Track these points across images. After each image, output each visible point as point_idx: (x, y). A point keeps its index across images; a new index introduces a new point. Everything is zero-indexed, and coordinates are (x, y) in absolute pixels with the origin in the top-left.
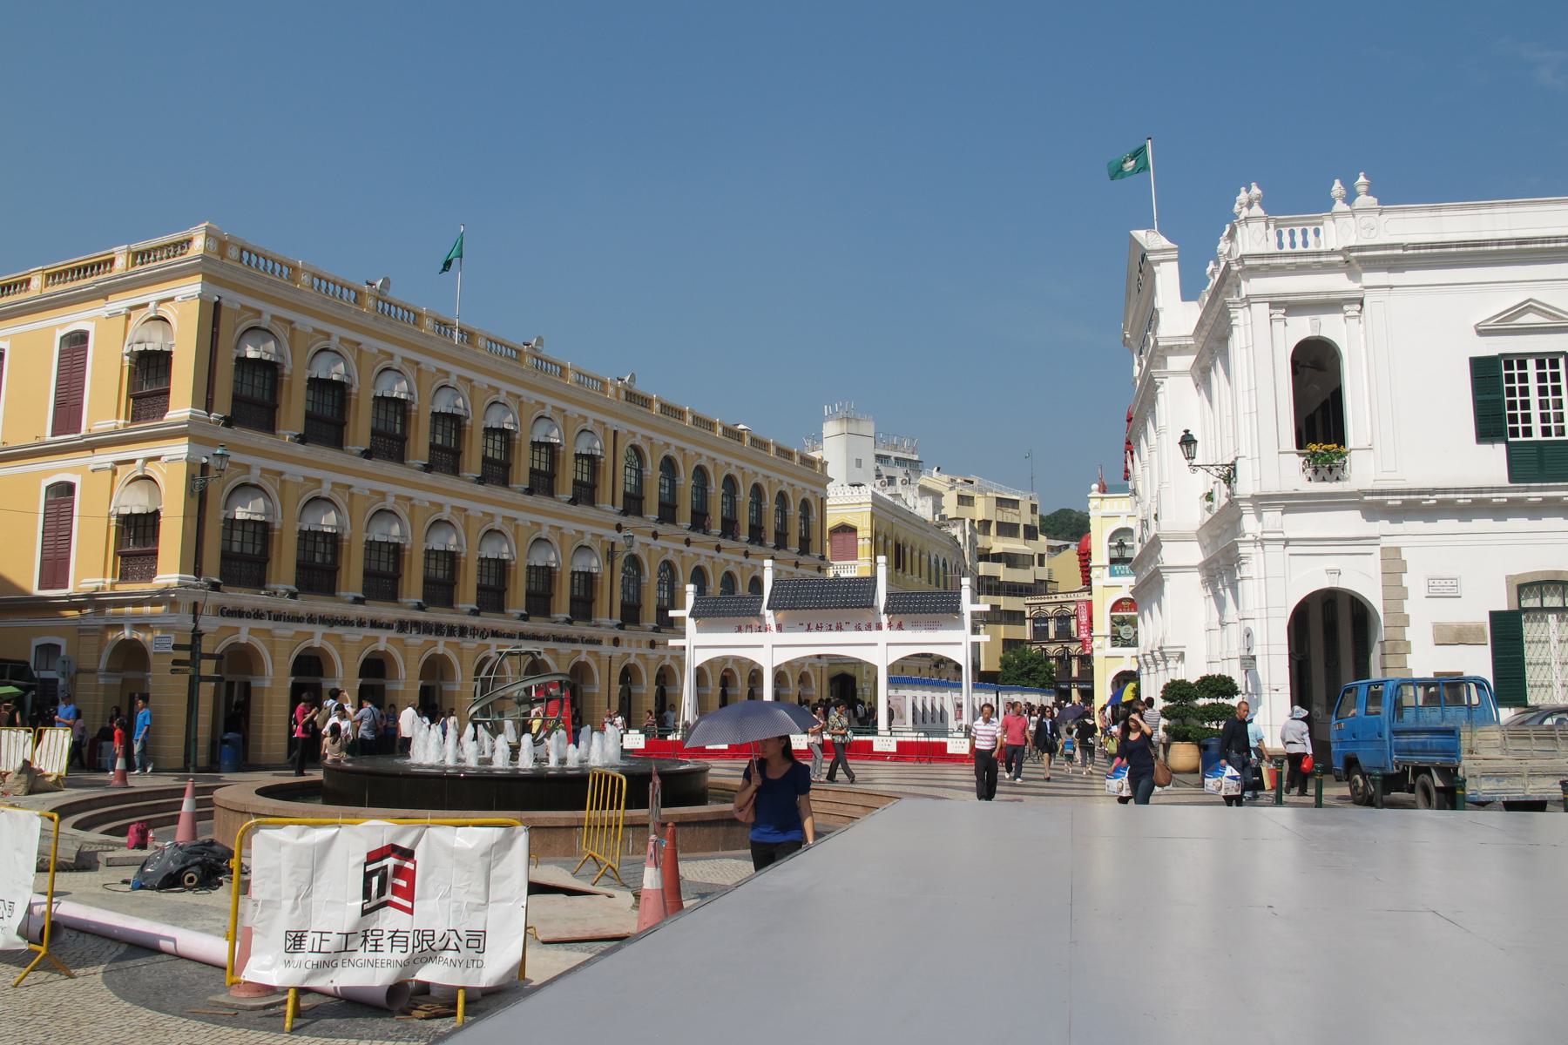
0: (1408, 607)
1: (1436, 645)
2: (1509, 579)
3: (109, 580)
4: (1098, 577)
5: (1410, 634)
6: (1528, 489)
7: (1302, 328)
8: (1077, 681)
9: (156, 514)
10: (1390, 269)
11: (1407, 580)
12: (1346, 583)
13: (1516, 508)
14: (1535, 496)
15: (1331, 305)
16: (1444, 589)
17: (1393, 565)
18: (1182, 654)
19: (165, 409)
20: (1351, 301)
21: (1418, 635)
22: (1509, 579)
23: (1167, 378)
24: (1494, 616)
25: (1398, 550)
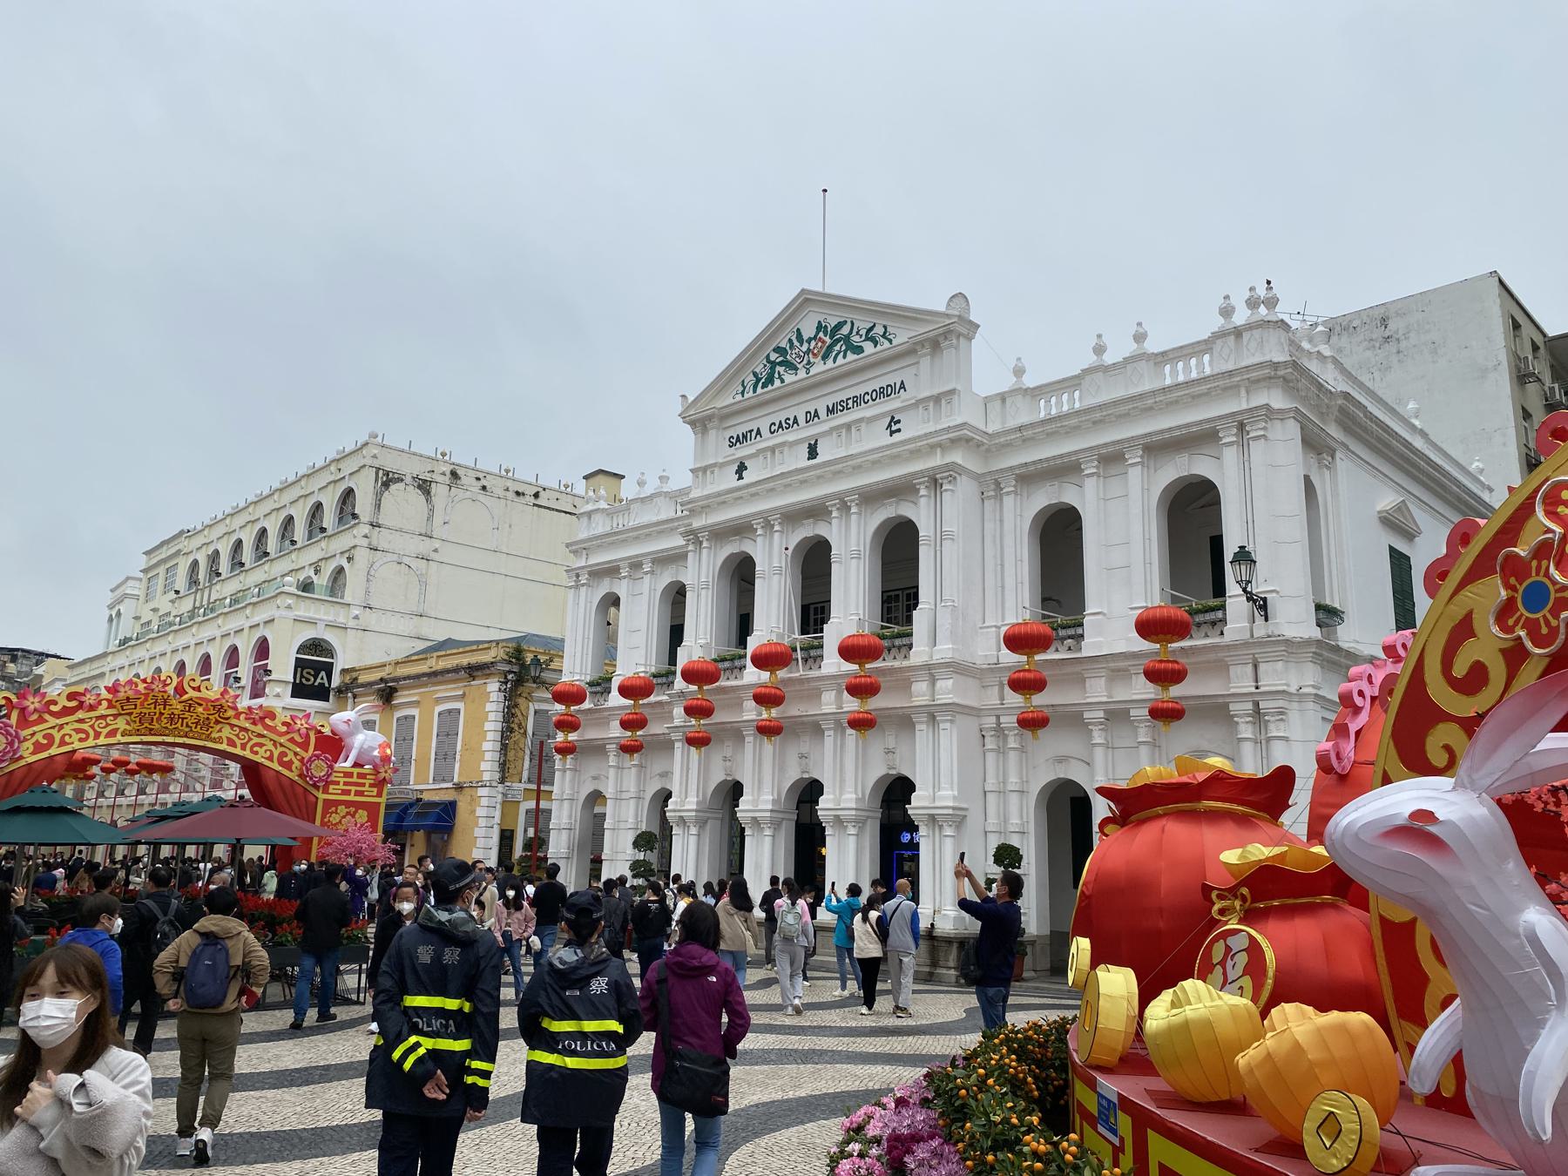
4: (278, 695)
23: (960, 474)
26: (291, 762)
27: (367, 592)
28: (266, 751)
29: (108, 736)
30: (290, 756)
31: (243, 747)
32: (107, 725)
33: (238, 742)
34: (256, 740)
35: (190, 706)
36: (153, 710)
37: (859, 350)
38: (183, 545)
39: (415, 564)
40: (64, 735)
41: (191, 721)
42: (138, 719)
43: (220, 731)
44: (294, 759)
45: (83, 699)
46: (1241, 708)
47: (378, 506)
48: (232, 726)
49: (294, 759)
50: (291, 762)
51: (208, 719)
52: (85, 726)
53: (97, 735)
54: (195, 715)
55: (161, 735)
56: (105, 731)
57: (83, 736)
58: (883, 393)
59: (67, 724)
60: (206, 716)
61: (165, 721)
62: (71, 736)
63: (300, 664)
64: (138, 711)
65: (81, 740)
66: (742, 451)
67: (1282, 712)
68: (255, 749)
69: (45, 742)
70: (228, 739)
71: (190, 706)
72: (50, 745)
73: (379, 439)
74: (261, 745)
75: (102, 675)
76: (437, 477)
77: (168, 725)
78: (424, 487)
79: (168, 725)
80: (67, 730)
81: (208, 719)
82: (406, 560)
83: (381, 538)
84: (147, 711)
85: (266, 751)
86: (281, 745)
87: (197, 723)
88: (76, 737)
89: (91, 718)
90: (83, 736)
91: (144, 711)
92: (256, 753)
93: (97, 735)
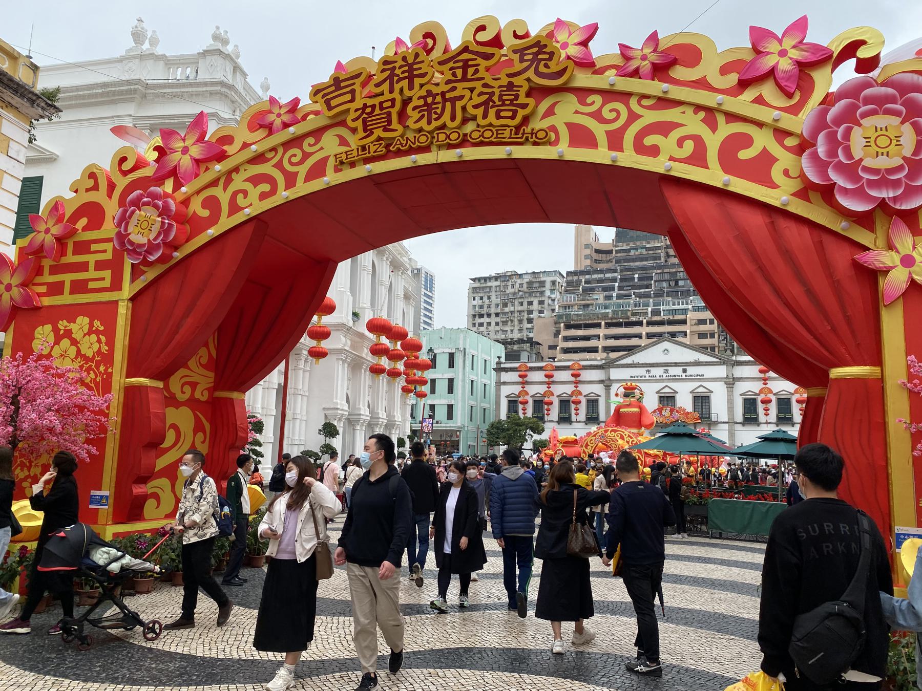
26: (766, 159)
28: (680, 143)
29: (309, 177)
30: (763, 140)
31: (615, 141)
32: (306, 156)
33: (599, 131)
34: (650, 117)
35: (466, 66)
36: (387, 96)
40: (235, 194)
41: (471, 101)
42: (359, 124)
43: (550, 112)
44: (775, 149)
45: (272, 117)
48: (583, 93)
49: (775, 149)
50: (766, 159)
51: (510, 86)
52: (266, 168)
53: (291, 180)
54: (478, 85)
55: (411, 151)
56: (303, 170)
57: (266, 187)
59: (236, 169)
60: (505, 81)
61: (415, 115)
62: (245, 193)
64: (358, 103)
65: (263, 196)
68: (649, 141)
69: (205, 213)
70: (572, 128)
71: (466, 66)
72: (214, 219)
74: (664, 128)
77: (423, 123)
79: (423, 123)
80: (239, 182)
81: (510, 86)
84: (376, 101)
85: (680, 143)
86: (732, 117)
87: (485, 103)
88: (254, 192)
89: (274, 149)
90: (266, 187)
91: (370, 102)
92: (654, 151)
93: (291, 180)
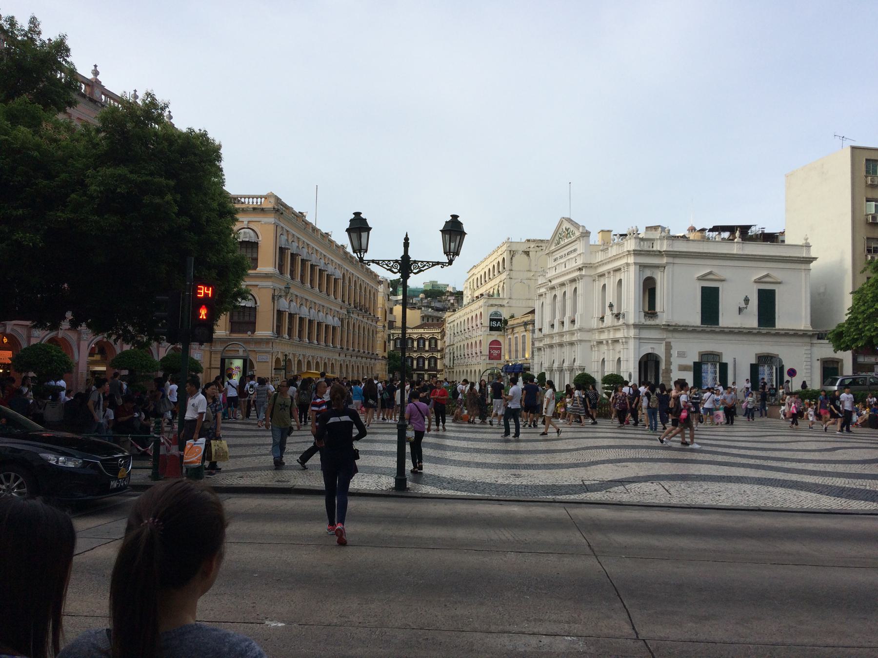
0: (672, 360)
1: (679, 370)
2: (699, 352)
3: (228, 332)
5: (672, 367)
6: (707, 327)
7: (648, 273)
8: (427, 370)
9: (255, 308)
10: (674, 257)
11: (672, 352)
12: (656, 352)
13: (703, 331)
14: (709, 329)
15: (657, 267)
16: (681, 355)
17: (668, 347)
18: (584, 369)
19: (257, 267)
20: (662, 267)
21: (674, 367)
22: (699, 352)
24: (695, 363)
25: (670, 342)
27: (511, 294)
37: (570, 237)
38: (475, 271)
39: (525, 281)
46: (620, 341)
47: (511, 263)
58: (575, 250)
63: (491, 320)
66: (555, 264)
67: (626, 342)
73: (510, 240)
75: (454, 321)
76: (531, 249)
78: (527, 253)
82: (523, 281)
83: (514, 275)
